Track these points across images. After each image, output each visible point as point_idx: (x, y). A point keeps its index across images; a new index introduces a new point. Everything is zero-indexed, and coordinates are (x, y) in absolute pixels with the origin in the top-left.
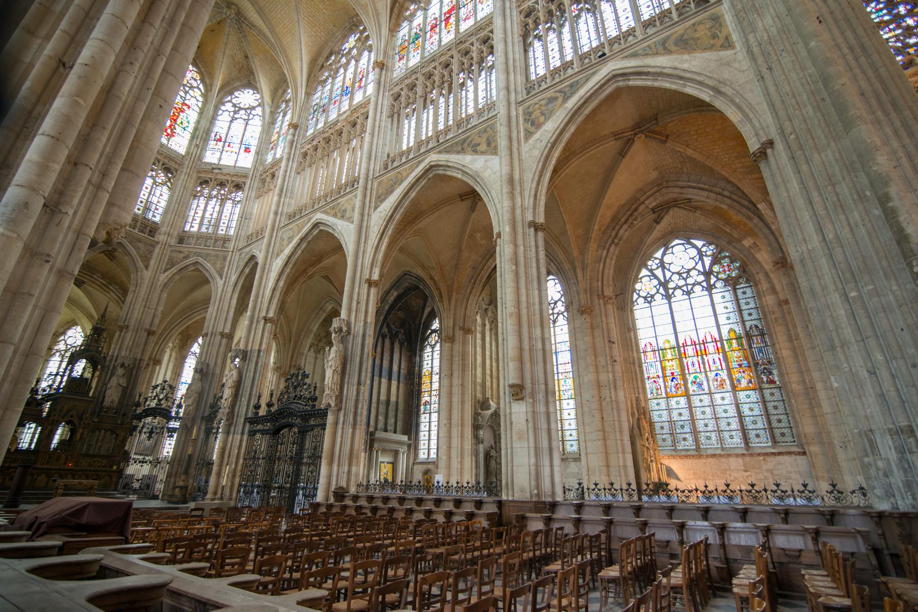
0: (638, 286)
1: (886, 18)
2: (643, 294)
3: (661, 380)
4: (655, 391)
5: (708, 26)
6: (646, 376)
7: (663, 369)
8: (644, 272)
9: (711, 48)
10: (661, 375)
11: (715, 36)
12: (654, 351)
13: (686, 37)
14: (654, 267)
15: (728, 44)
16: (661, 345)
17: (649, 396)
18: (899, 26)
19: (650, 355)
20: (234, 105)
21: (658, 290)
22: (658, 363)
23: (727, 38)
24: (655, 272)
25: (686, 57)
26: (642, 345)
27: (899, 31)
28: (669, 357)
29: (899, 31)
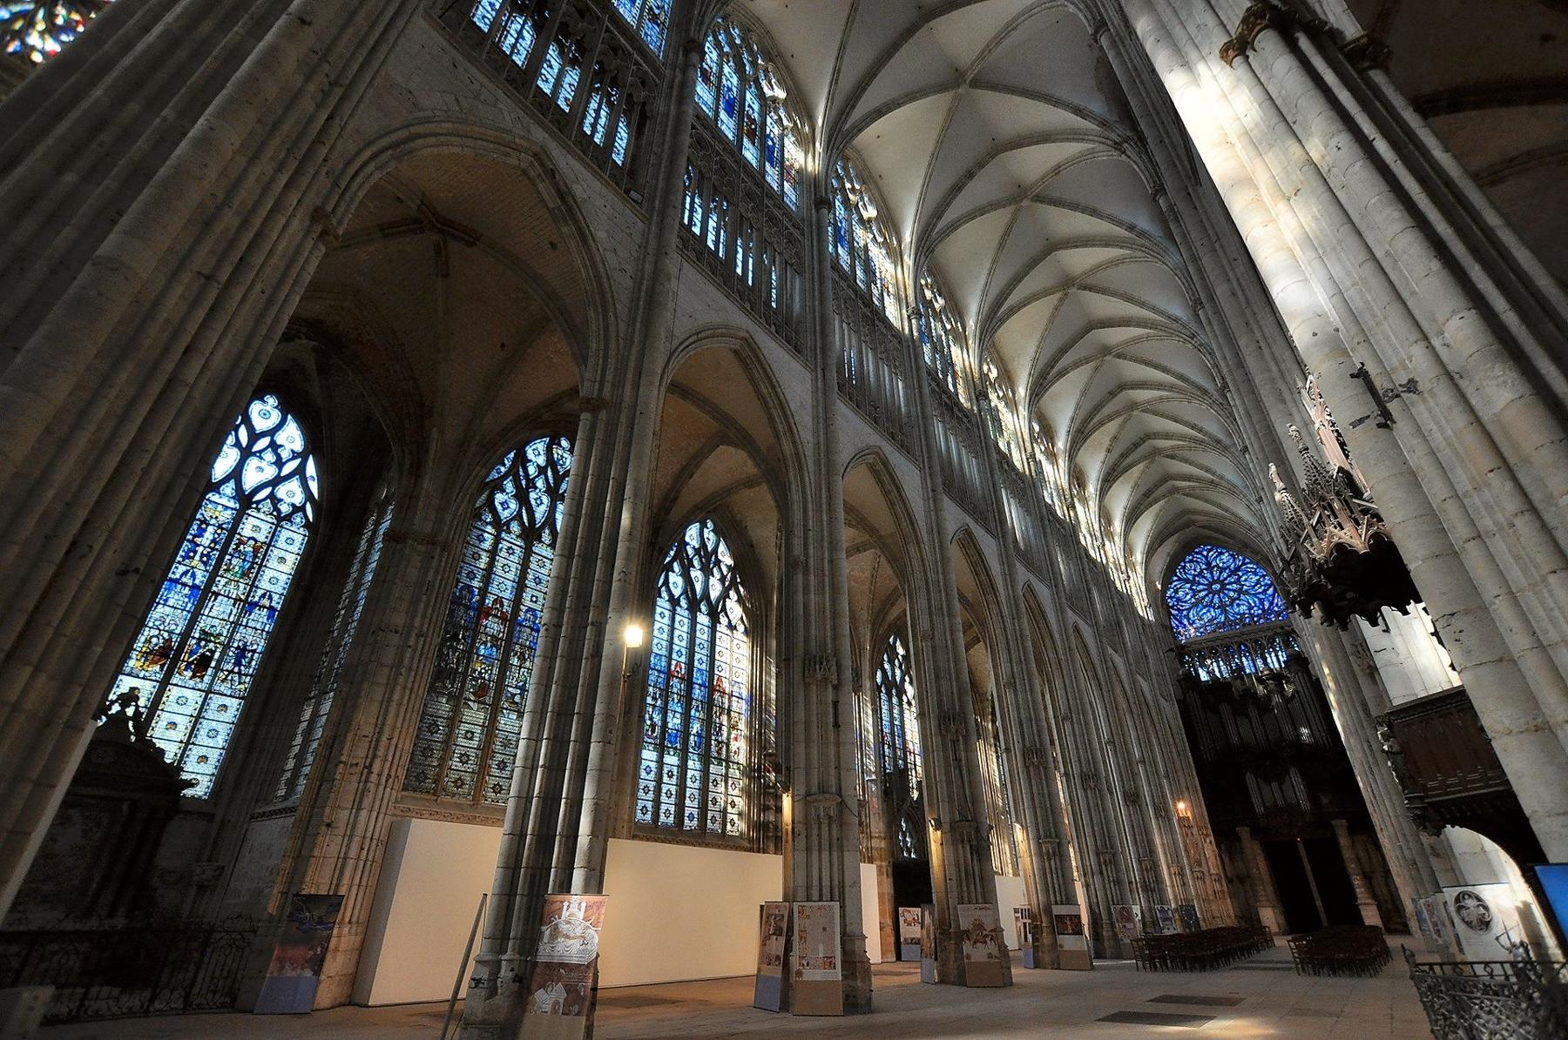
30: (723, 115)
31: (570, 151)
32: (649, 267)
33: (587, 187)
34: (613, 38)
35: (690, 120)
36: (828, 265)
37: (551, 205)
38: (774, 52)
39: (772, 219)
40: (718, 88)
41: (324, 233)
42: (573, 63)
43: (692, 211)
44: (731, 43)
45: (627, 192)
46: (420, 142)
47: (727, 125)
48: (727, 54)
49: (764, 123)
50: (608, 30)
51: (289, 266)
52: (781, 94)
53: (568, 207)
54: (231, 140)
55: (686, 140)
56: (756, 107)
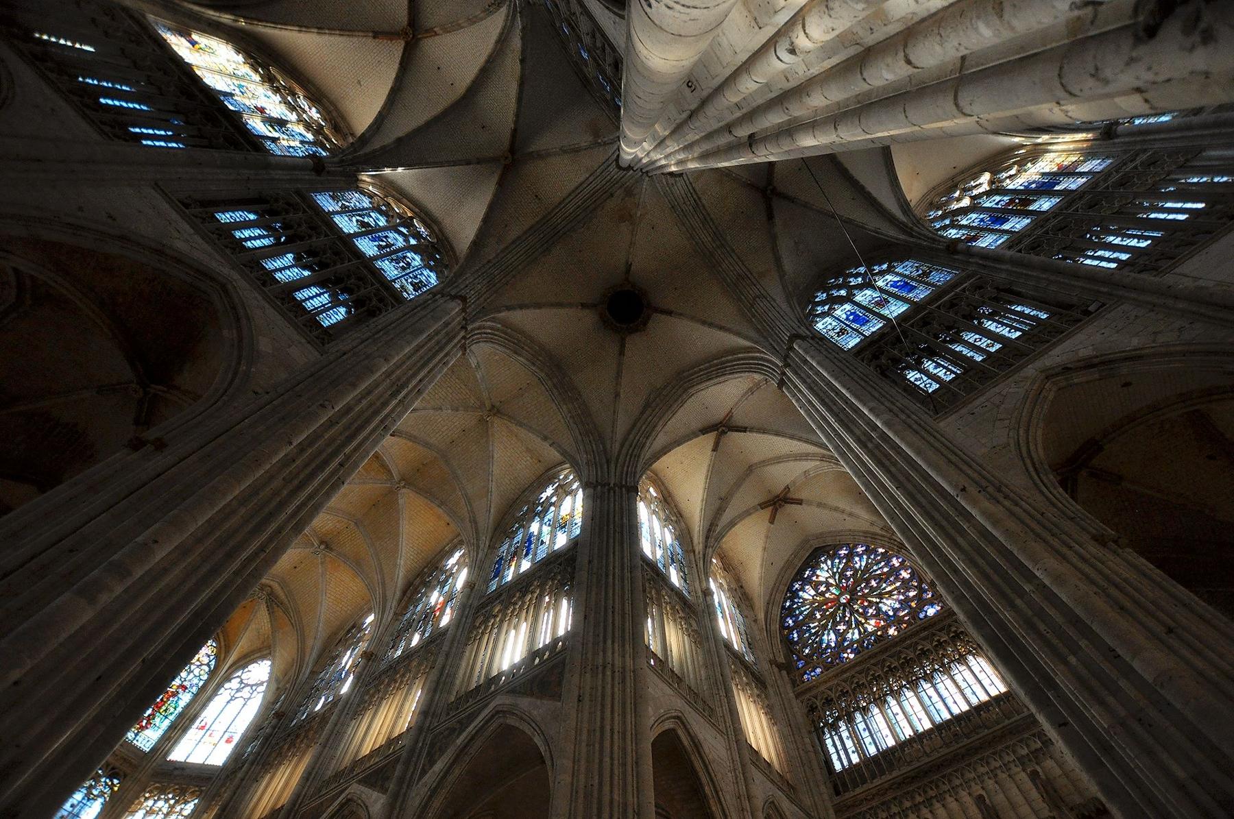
1: (886, 570)
18: (897, 579)
20: (241, 682)
25: (539, 702)
27: (898, 584)
29: (898, 584)
30: (1006, 227)
31: (1042, 354)
32: (1181, 305)
33: (1082, 343)
34: (944, 305)
35: (1009, 253)
36: (1195, 120)
37: (1097, 376)
38: (950, 184)
39: (1122, 183)
40: (982, 229)
41: (1115, 542)
42: (957, 333)
43: (1101, 259)
44: (943, 217)
45: (1087, 313)
46: (1034, 455)
47: (1017, 224)
48: (952, 221)
49: (1014, 191)
50: (938, 307)
51: (1145, 575)
52: (986, 177)
53: (1101, 364)
54: (1052, 562)
55: (1034, 258)
56: (998, 198)
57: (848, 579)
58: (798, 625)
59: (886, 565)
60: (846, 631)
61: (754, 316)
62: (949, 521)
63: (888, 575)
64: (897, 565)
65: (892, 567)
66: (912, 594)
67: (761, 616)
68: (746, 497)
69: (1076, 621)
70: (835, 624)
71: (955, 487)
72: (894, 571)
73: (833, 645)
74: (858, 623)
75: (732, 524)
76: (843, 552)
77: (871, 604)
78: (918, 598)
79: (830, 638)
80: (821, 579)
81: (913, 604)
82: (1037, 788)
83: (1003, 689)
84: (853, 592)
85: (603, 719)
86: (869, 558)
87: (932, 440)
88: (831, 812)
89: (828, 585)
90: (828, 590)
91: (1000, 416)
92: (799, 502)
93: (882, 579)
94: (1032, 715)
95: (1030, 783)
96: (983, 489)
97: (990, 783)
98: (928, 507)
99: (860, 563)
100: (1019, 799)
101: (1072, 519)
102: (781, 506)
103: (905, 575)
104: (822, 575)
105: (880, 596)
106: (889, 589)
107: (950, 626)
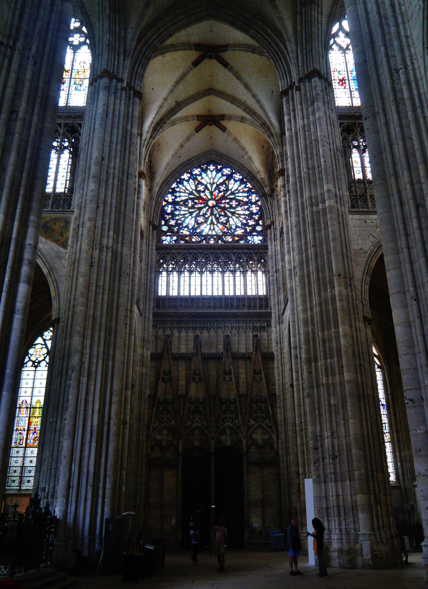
0: (31, 351)
1: (245, 200)
2: (33, 358)
3: (25, 433)
4: (18, 441)
5: (62, 225)
6: (15, 428)
7: (30, 424)
8: (40, 340)
9: (57, 241)
10: (26, 429)
11: (61, 235)
12: (27, 408)
13: (48, 225)
14: (48, 338)
15: (65, 246)
16: (34, 404)
17: (13, 445)
18: (248, 209)
19: (23, 411)
21: (45, 358)
22: (27, 419)
23: (67, 239)
24: (47, 342)
26: (20, 402)
28: (37, 415)
29: (247, 212)
57: (220, 192)
58: (174, 203)
59: (247, 197)
60: (202, 223)
61: (301, 14)
62: (324, 284)
63: (246, 203)
64: (253, 201)
65: (250, 201)
66: (251, 223)
67: (156, 189)
68: (194, 109)
69: (339, 350)
70: (198, 215)
71: (338, 272)
72: (249, 202)
73: (190, 227)
74: (212, 223)
75: (174, 123)
76: (227, 171)
77: (226, 215)
78: (254, 227)
79: (190, 221)
80: (203, 181)
81: (248, 229)
82: (253, 341)
83: (262, 292)
84: (219, 201)
85: (104, 281)
86: (240, 186)
87: (342, 229)
88: (151, 315)
89: (206, 188)
90: (204, 192)
91: (374, 234)
92: (224, 129)
93: (240, 203)
94: (271, 313)
95: (251, 338)
96: (345, 277)
97: (235, 332)
98: (320, 267)
99: (233, 186)
100: (243, 342)
101: (363, 304)
102: (211, 125)
103: (254, 209)
104: (206, 179)
105: (233, 213)
106: (241, 212)
107: (261, 254)
